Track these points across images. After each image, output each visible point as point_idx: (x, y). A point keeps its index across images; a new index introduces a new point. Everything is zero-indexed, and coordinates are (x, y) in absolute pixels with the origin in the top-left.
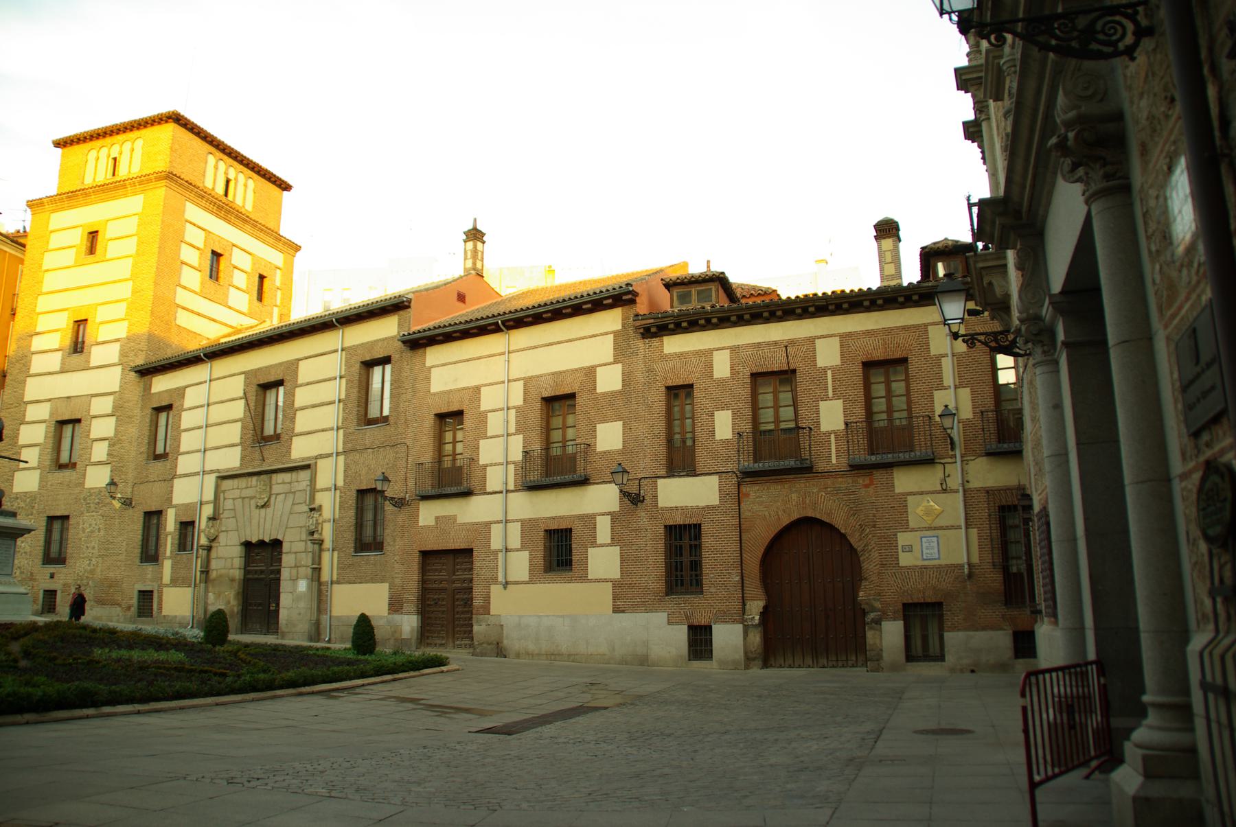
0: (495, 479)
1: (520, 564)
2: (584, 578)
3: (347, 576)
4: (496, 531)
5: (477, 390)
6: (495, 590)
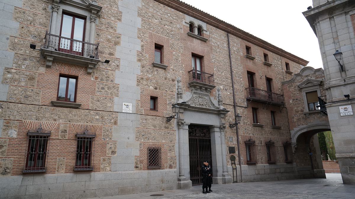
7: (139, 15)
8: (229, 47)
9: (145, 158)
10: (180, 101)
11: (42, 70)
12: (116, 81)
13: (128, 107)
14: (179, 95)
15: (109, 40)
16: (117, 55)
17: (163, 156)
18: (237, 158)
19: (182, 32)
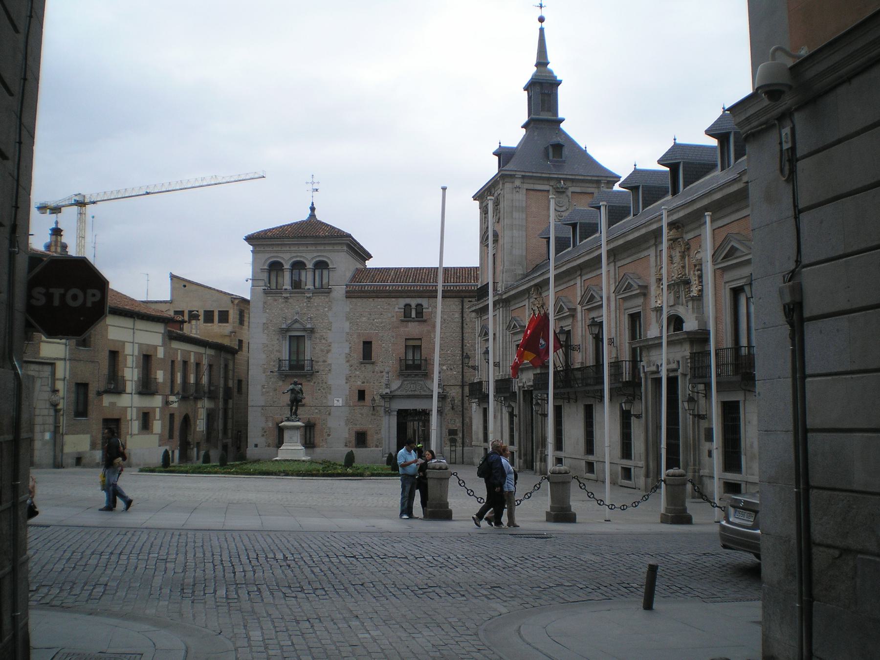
0: (130, 387)
1: (135, 426)
2: (152, 433)
3: (74, 431)
4: (129, 410)
5: (124, 343)
6: (128, 437)
7: (348, 319)
8: (462, 317)
9: (353, 439)
10: (388, 391)
11: (281, 383)
12: (329, 383)
13: (338, 402)
14: (387, 386)
15: (322, 351)
16: (329, 361)
17: (369, 438)
18: (459, 441)
19: (394, 319)
